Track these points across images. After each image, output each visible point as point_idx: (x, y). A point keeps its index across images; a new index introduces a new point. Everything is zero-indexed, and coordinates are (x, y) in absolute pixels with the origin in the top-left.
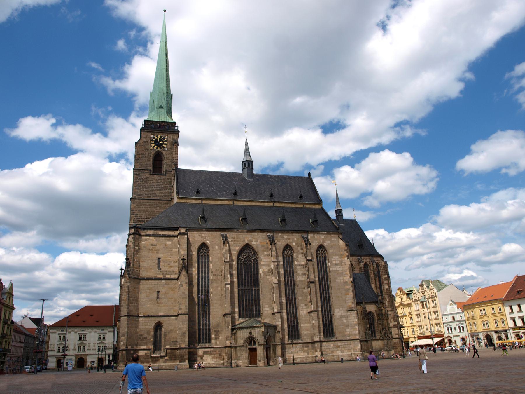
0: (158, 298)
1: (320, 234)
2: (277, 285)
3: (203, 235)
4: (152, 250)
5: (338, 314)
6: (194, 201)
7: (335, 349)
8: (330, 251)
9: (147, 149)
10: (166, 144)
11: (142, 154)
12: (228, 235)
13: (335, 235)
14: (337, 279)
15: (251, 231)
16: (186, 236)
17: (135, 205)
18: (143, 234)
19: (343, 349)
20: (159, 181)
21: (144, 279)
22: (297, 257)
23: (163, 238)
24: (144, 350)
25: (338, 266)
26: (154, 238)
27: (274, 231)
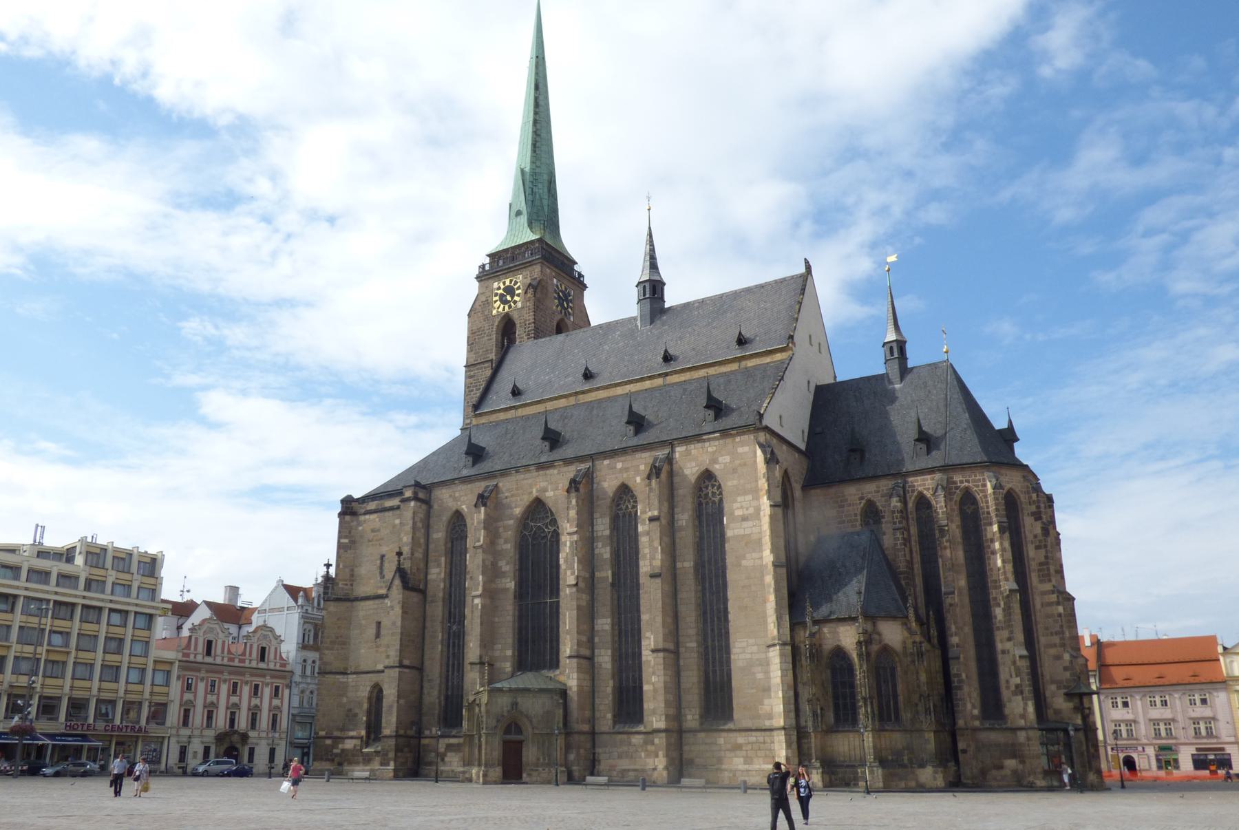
0: (378, 635)
1: (704, 441)
2: (574, 589)
5: (741, 656)
8: (729, 484)
13: (745, 437)
14: (744, 558)
19: (750, 753)
22: (644, 512)
23: (390, 513)
24: (352, 738)
25: (750, 523)
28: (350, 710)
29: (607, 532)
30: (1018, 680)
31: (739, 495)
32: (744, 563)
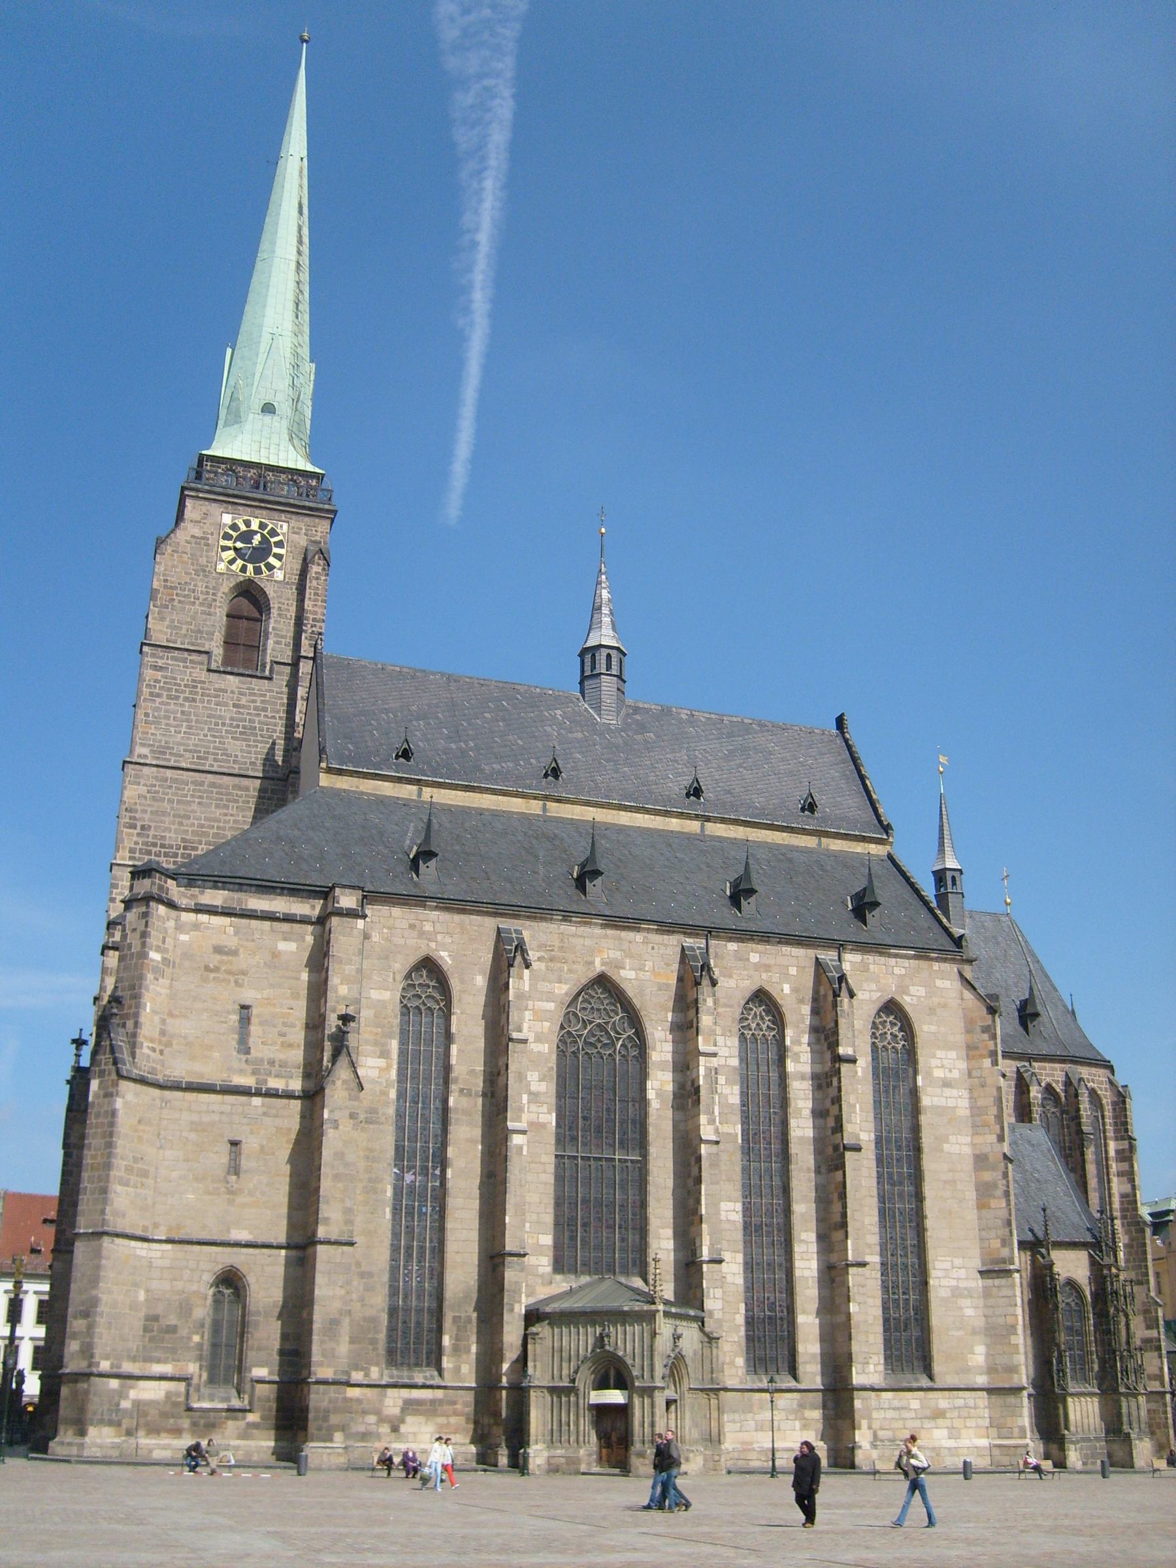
1: (890, 955)
3: (428, 927)
4: (216, 969)
5: (944, 1282)
6: (387, 789)
7: (928, 1424)
8: (925, 1028)
9: (203, 571)
10: (279, 557)
11: (183, 585)
12: (526, 935)
13: (946, 966)
15: (616, 922)
16: (360, 923)
17: (142, 790)
18: (183, 902)
19: (957, 1423)
20: (243, 701)
21: (176, 1087)
23: (267, 924)
24: (162, 1378)
25: (954, 1092)
26: (226, 920)
27: (710, 932)
28: (153, 1318)
29: (735, 1062)
30: (1153, 1333)
31: (939, 1048)
32: (946, 1147)
